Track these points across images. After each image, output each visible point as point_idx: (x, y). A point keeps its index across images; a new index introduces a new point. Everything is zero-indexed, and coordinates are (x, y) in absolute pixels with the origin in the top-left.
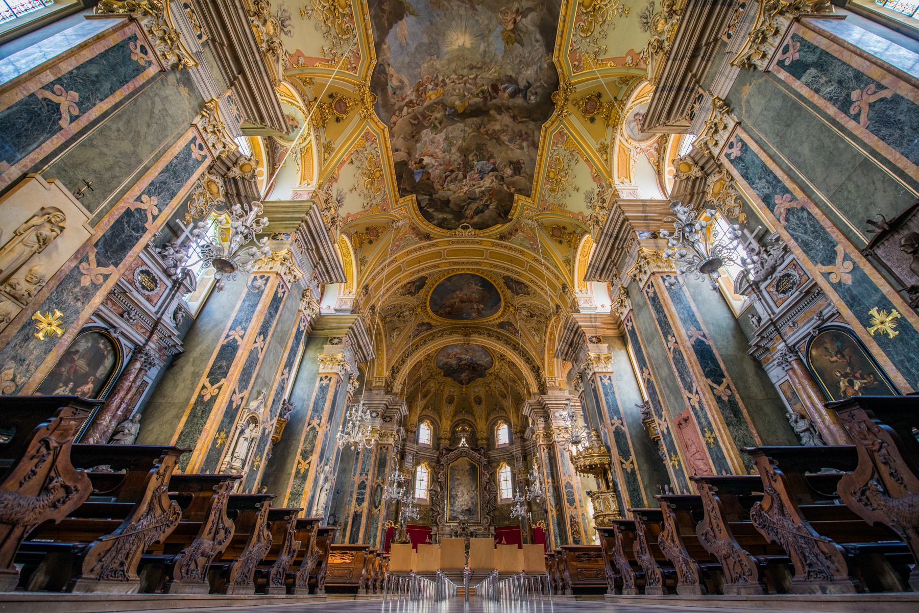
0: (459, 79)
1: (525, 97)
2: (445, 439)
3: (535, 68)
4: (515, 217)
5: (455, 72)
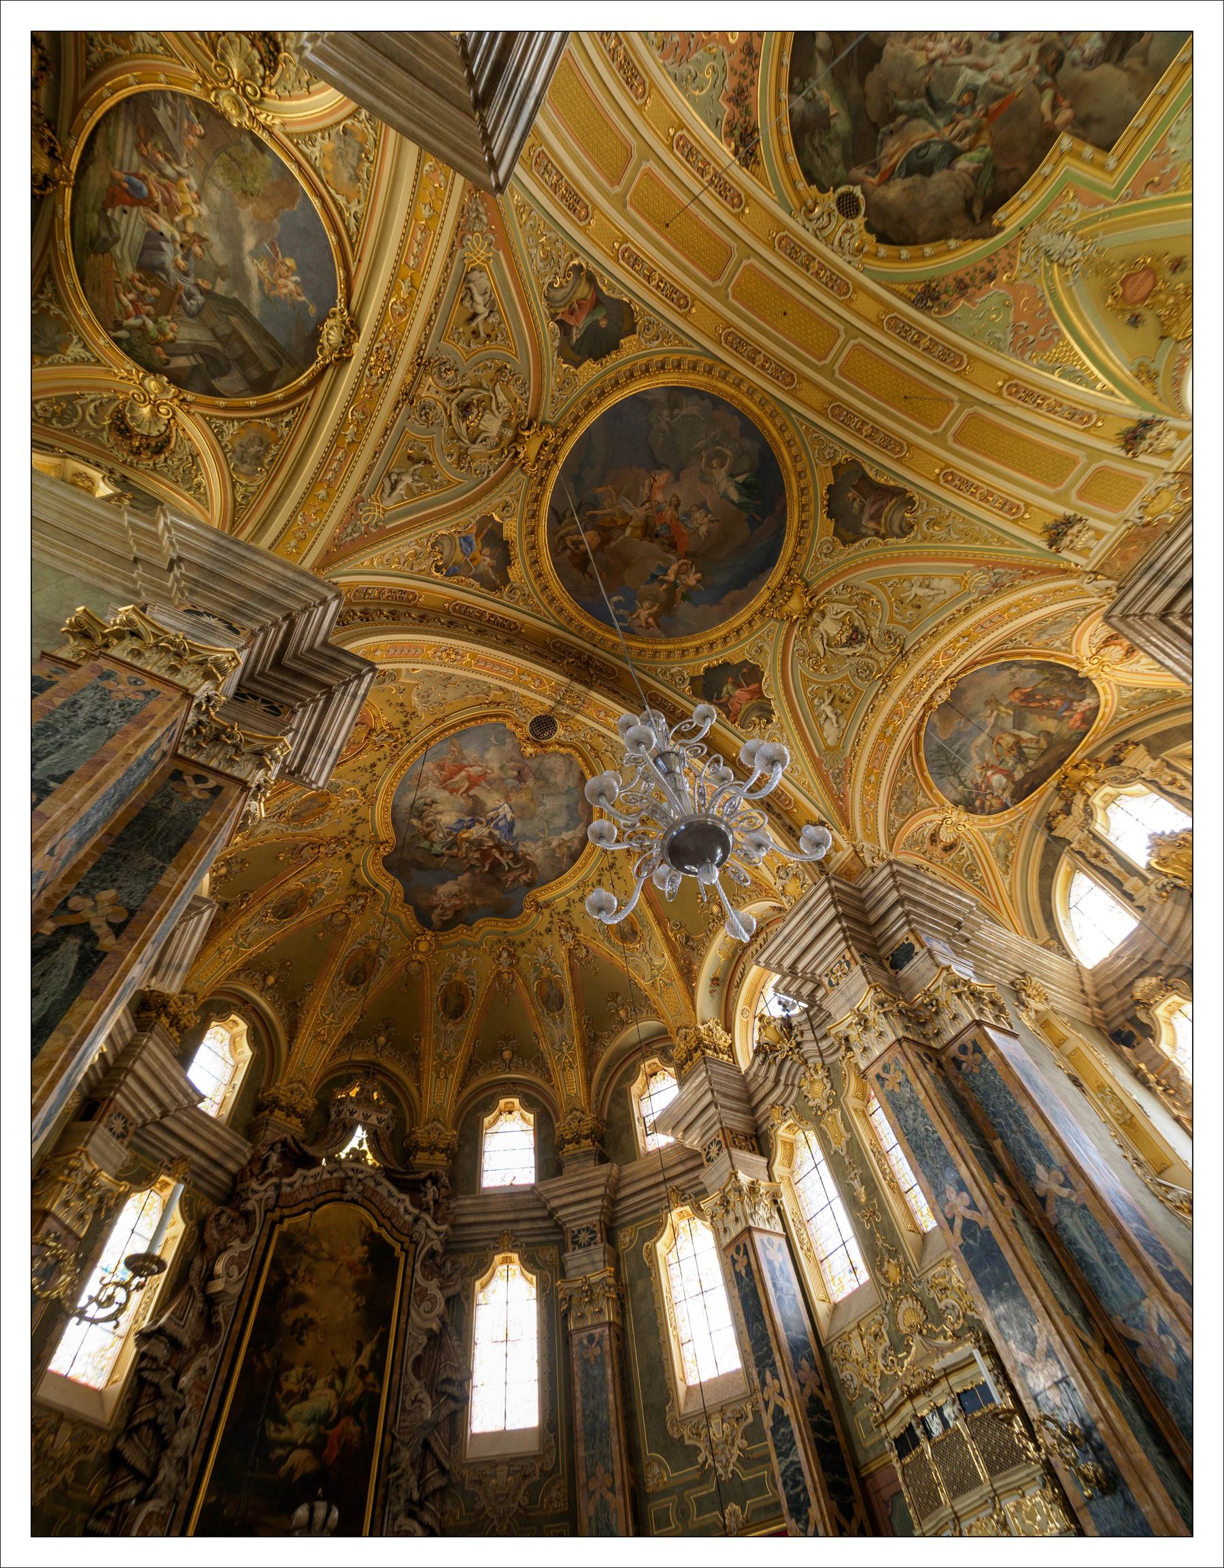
2: (291, 1111)
4: (1011, 226)
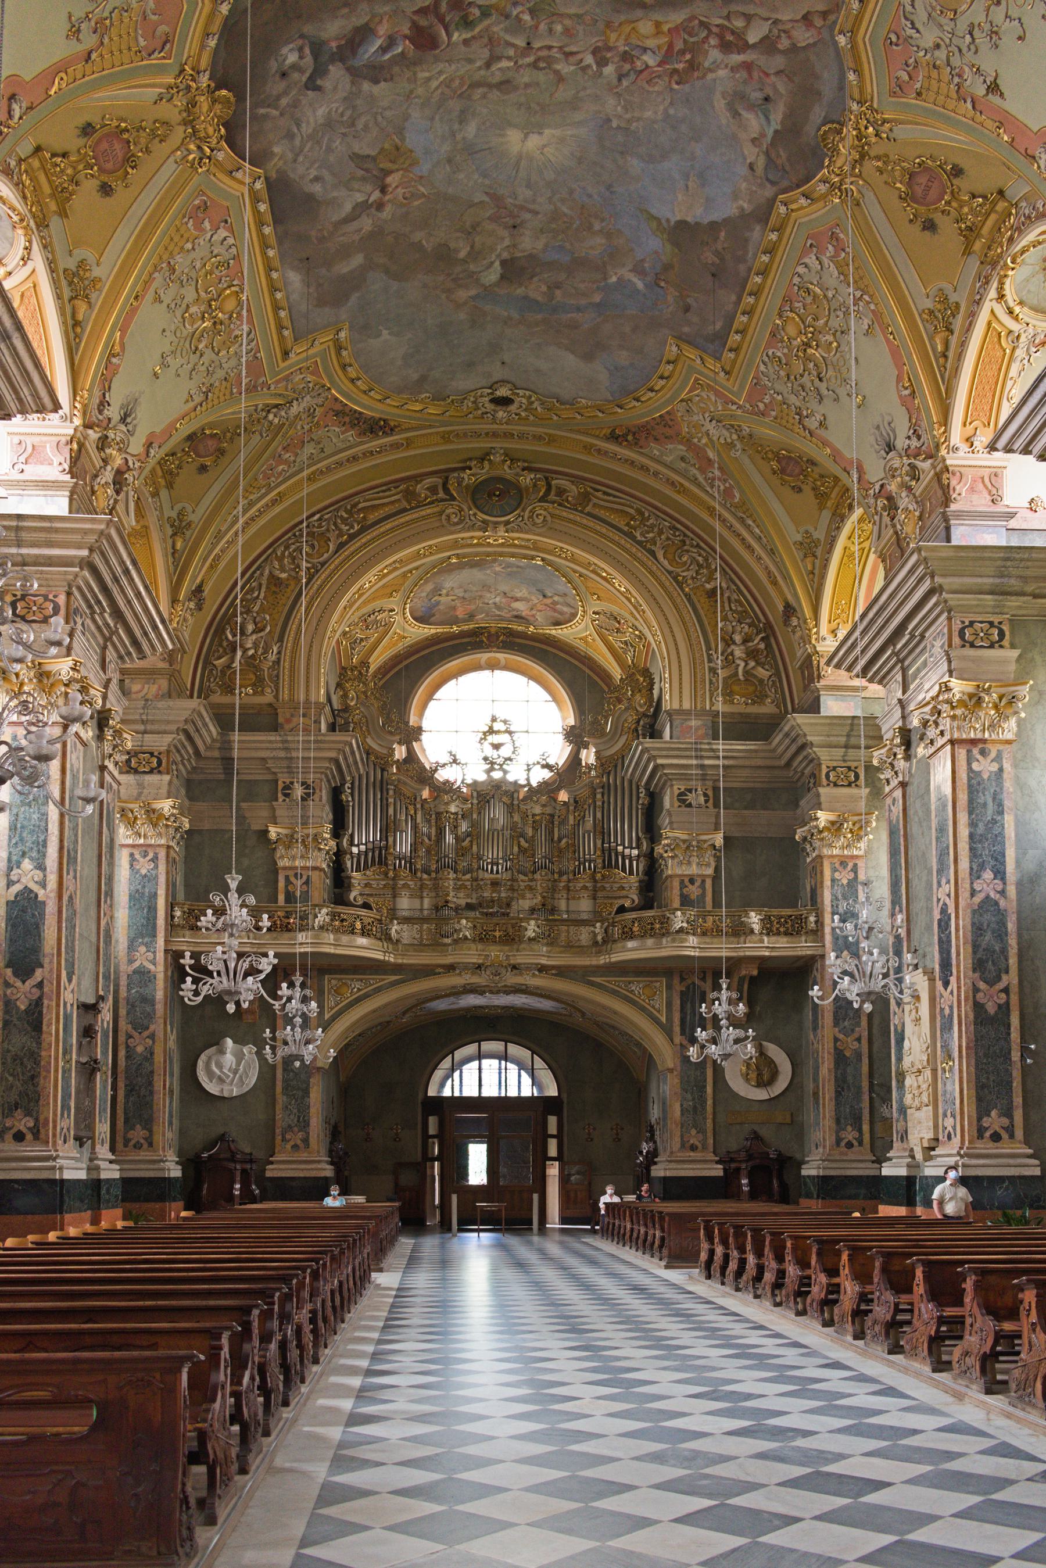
0: (550, 61)
1: (317, 48)
3: (306, 129)
5: (560, 78)
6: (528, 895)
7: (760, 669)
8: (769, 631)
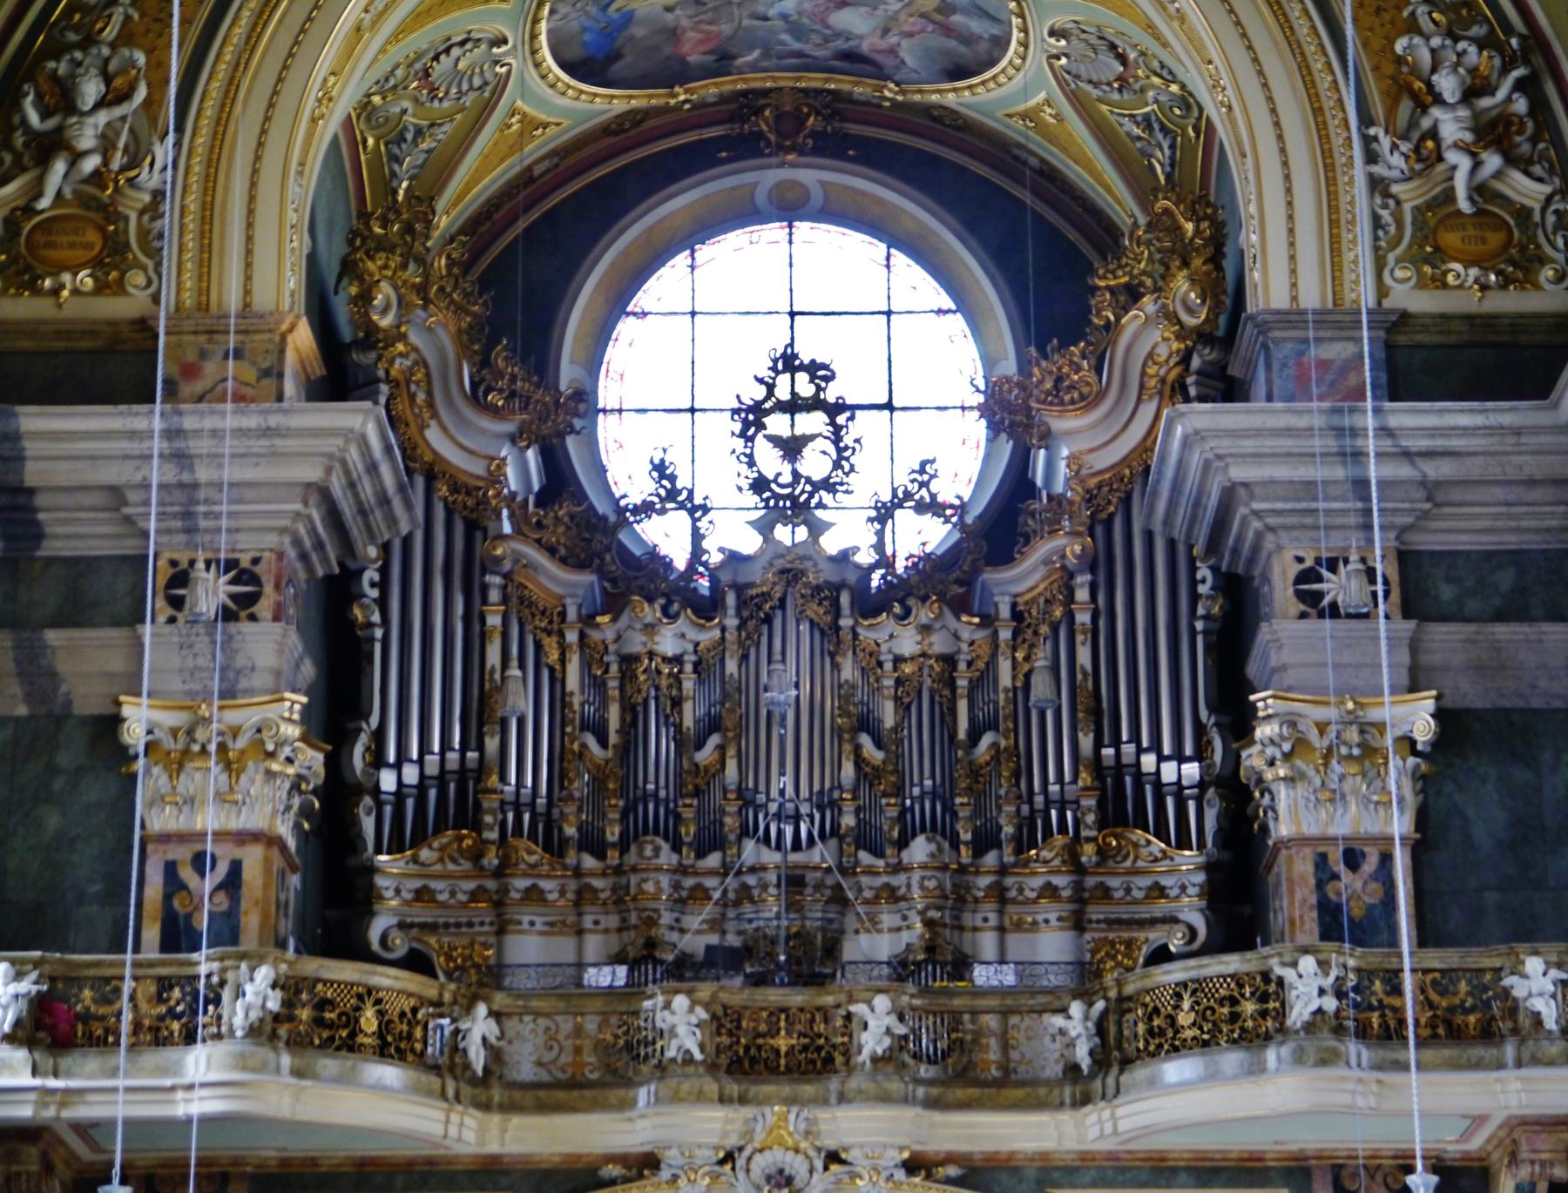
6: (888, 919)
7: (1517, 177)
8: (1538, 60)
